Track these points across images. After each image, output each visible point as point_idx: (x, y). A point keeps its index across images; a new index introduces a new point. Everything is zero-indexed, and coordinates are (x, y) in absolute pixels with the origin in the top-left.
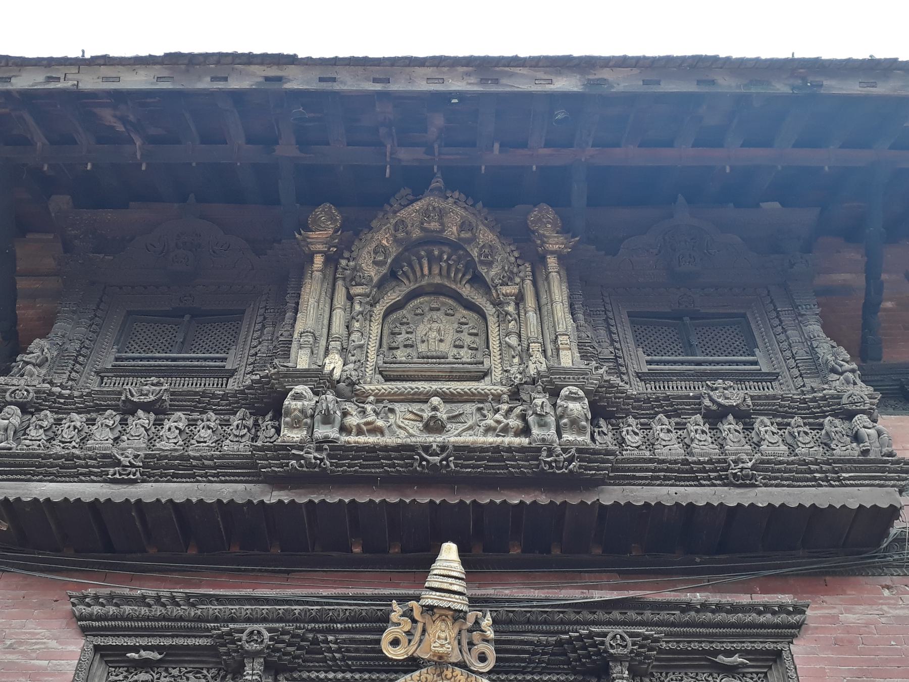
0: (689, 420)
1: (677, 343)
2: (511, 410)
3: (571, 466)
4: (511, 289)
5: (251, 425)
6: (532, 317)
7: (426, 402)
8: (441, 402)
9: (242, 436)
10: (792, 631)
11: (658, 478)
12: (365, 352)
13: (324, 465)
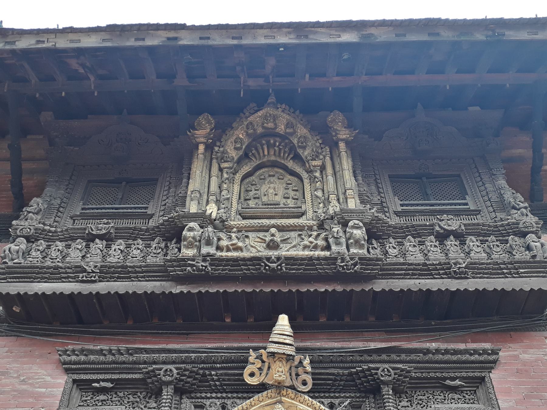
0: (426, 239)
1: (418, 193)
2: (318, 235)
3: (356, 268)
4: (318, 163)
5: (164, 246)
6: (331, 179)
7: (267, 231)
8: (277, 231)
9: (158, 254)
10: (491, 365)
11: (408, 274)
12: (230, 202)
13: (207, 270)
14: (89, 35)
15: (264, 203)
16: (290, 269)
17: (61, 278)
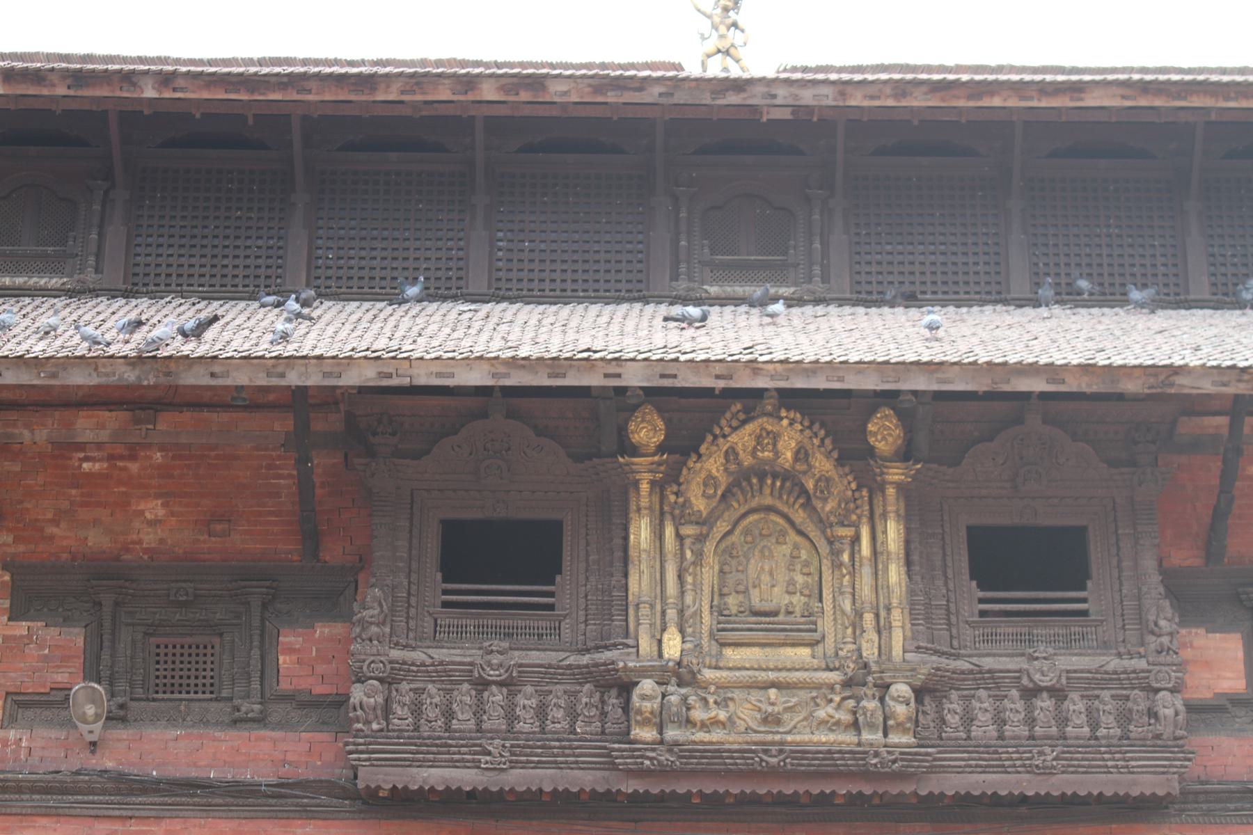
2: (844, 699)
6: (866, 571)
11: (971, 766)
17: (452, 761)
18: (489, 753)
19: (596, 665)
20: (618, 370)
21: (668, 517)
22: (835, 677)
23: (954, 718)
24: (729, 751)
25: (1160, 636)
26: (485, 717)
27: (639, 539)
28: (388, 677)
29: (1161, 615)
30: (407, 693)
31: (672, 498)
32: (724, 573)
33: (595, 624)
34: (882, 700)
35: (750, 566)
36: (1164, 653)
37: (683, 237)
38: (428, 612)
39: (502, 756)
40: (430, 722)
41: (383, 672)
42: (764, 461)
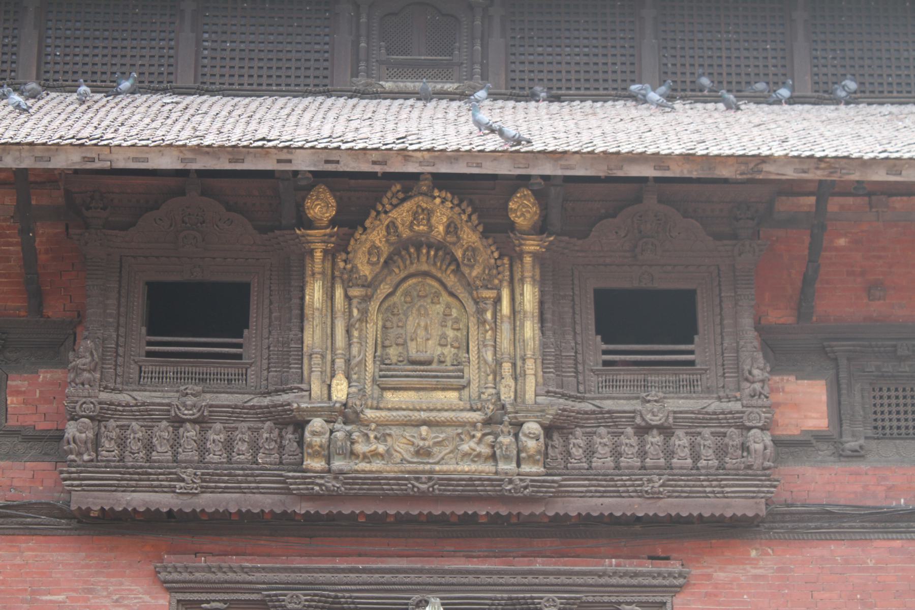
2: (484, 435)
4: (491, 294)
6: (506, 328)
10: (675, 590)
11: (591, 492)
14: (160, 151)
15: (410, 359)
16: (445, 490)
17: (151, 486)
18: (183, 480)
19: (275, 406)
20: (289, 157)
21: (338, 280)
22: (477, 416)
23: (578, 451)
24: (386, 478)
25: (753, 382)
26: (180, 450)
27: (313, 300)
28: (98, 416)
29: (755, 366)
30: (114, 429)
31: (342, 265)
32: (387, 328)
33: (276, 371)
34: (516, 436)
35: (409, 323)
36: (757, 397)
37: (363, 39)
38: (134, 360)
39: (194, 482)
40: (133, 454)
41: (93, 412)
42: (419, 234)
